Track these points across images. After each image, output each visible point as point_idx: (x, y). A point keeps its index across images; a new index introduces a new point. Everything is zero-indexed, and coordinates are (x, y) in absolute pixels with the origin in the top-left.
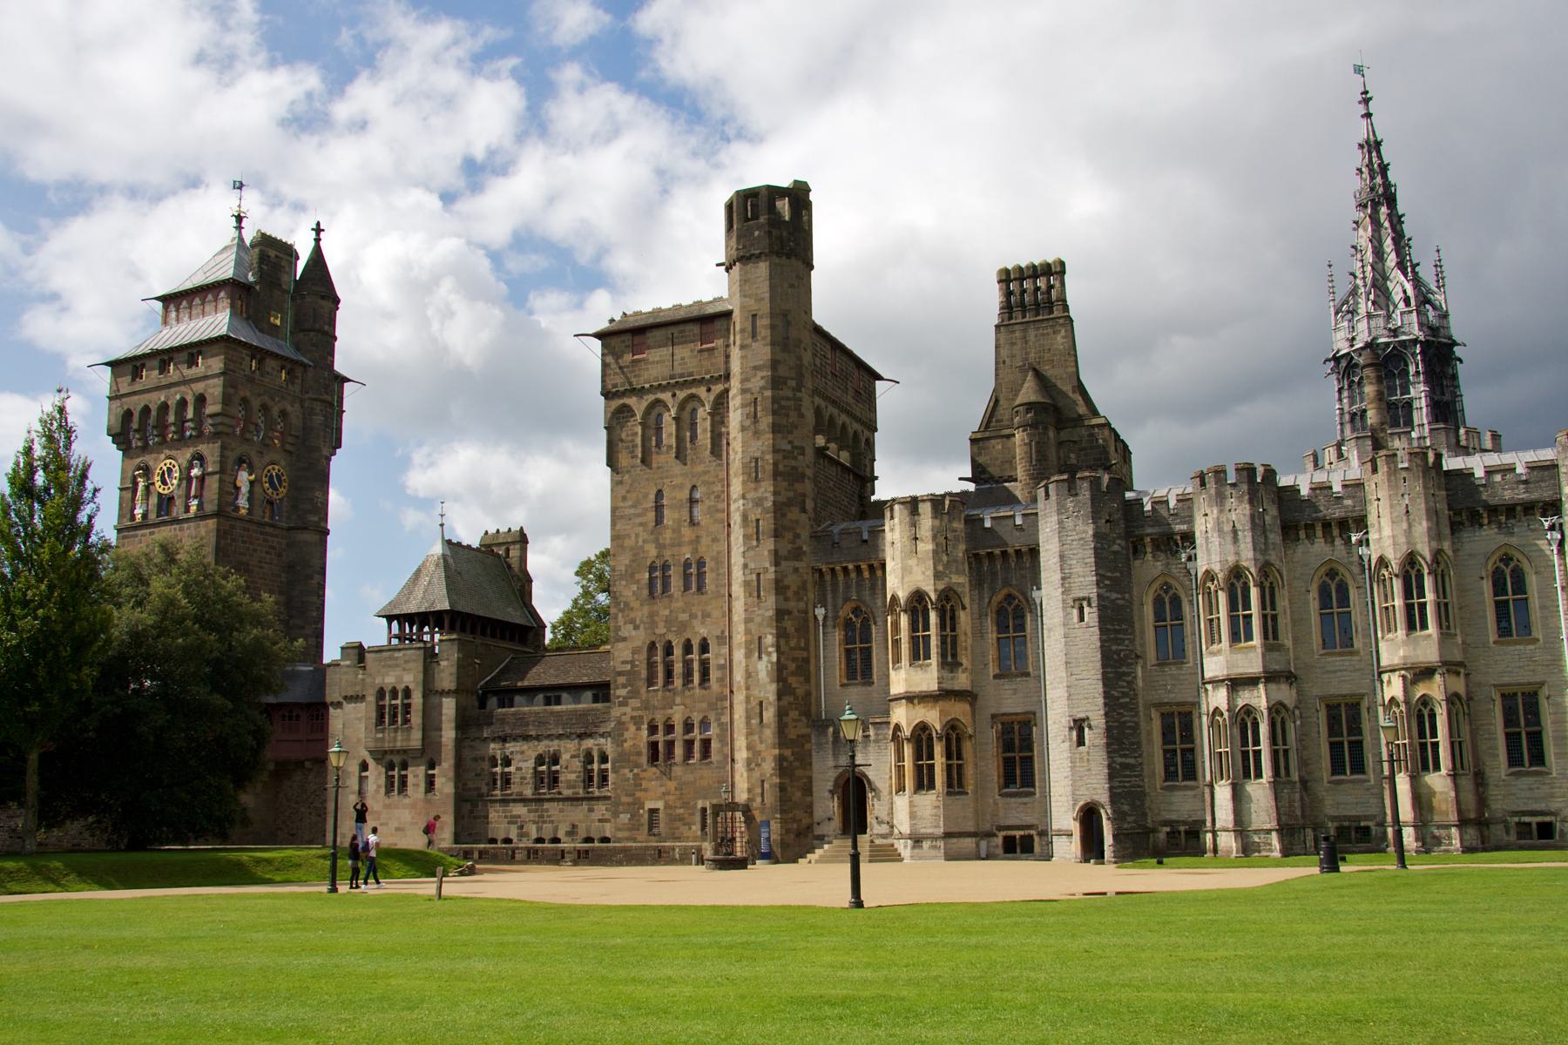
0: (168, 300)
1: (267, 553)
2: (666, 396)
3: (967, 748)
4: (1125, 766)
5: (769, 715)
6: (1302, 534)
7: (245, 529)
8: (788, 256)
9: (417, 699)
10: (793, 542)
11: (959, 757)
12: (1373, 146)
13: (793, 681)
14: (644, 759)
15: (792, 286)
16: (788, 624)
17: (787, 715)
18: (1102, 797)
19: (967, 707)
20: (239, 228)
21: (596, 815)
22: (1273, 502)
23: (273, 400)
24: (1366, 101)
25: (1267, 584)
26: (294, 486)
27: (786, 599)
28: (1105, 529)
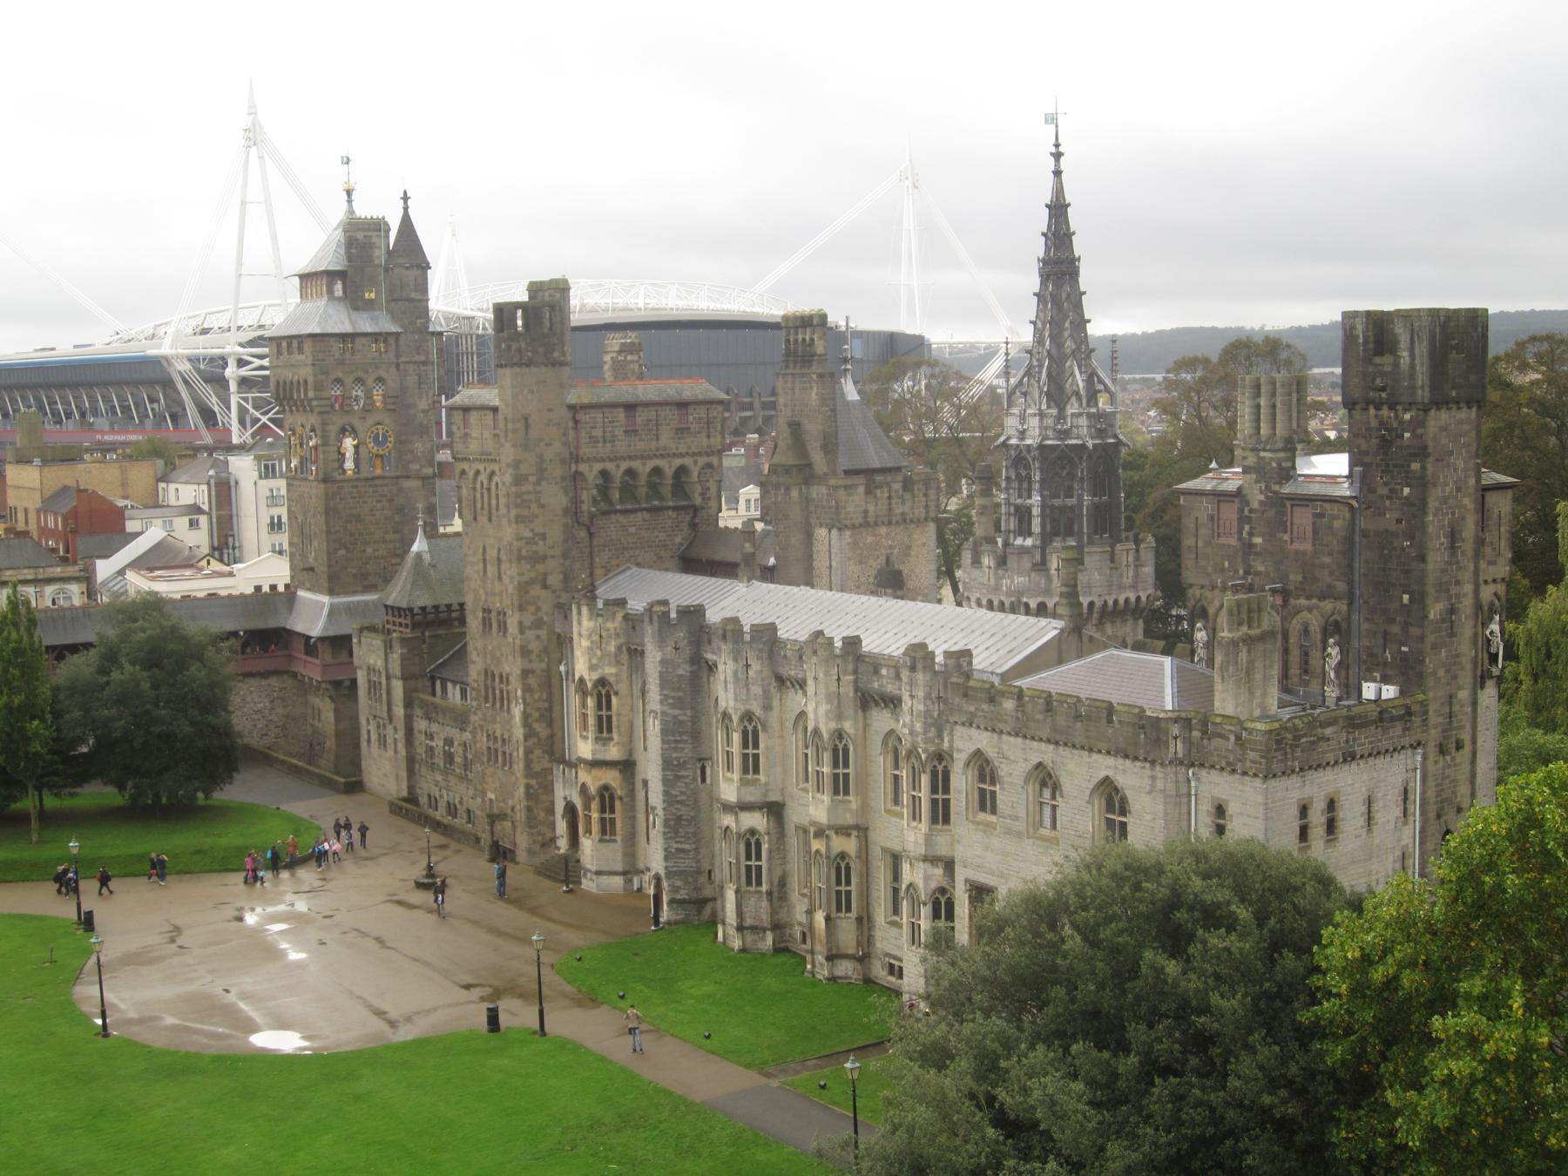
0: (305, 278)
1: (378, 501)
3: (618, 804)
4: (677, 849)
5: (521, 751)
6: (788, 683)
7: (353, 487)
8: (528, 365)
9: (384, 681)
10: (534, 614)
11: (612, 811)
12: (1058, 209)
13: (536, 726)
14: (485, 759)
15: (531, 392)
16: (532, 681)
17: (532, 752)
18: (662, 873)
20: (350, 201)
21: (471, 792)
22: (758, 658)
23: (367, 372)
24: (1057, 156)
25: (750, 728)
26: (400, 442)
27: (530, 661)
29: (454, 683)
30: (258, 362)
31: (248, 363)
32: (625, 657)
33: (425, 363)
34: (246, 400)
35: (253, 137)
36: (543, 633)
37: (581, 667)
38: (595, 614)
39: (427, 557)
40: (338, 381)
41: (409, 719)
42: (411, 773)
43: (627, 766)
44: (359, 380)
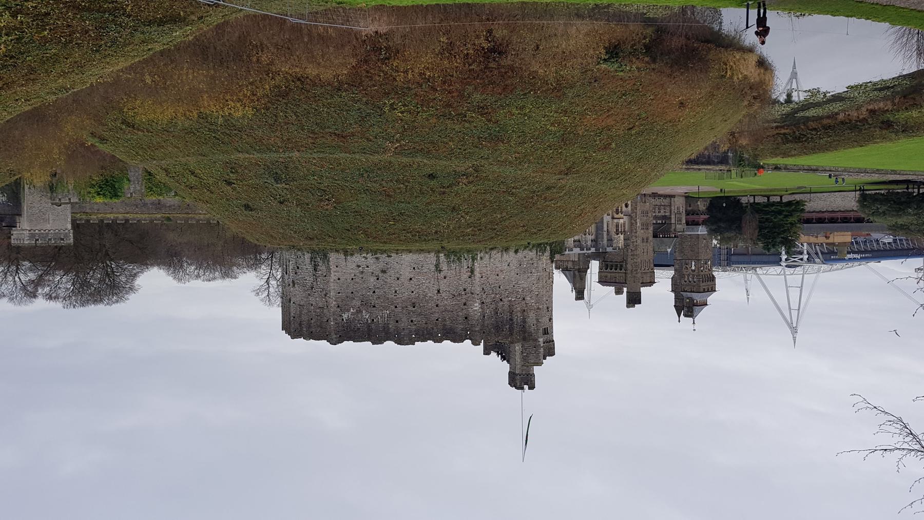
0: (707, 305)
2: (647, 271)
19: (615, 217)
20: (694, 321)
28: (601, 243)
29: (659, 224)
30: (796, 259)
31: (799, 259)
32: (613, 239)
33: (675, 285)
34: (801, 248)
35: (794, 330)
36: (632, 241)
37: (622, 237)
38: (619, 247)
39: (667, 247)
40: (695, 282)
41: (671, 215)
42: (671, 203)
43: (613, 218)
44: (690, 282)
